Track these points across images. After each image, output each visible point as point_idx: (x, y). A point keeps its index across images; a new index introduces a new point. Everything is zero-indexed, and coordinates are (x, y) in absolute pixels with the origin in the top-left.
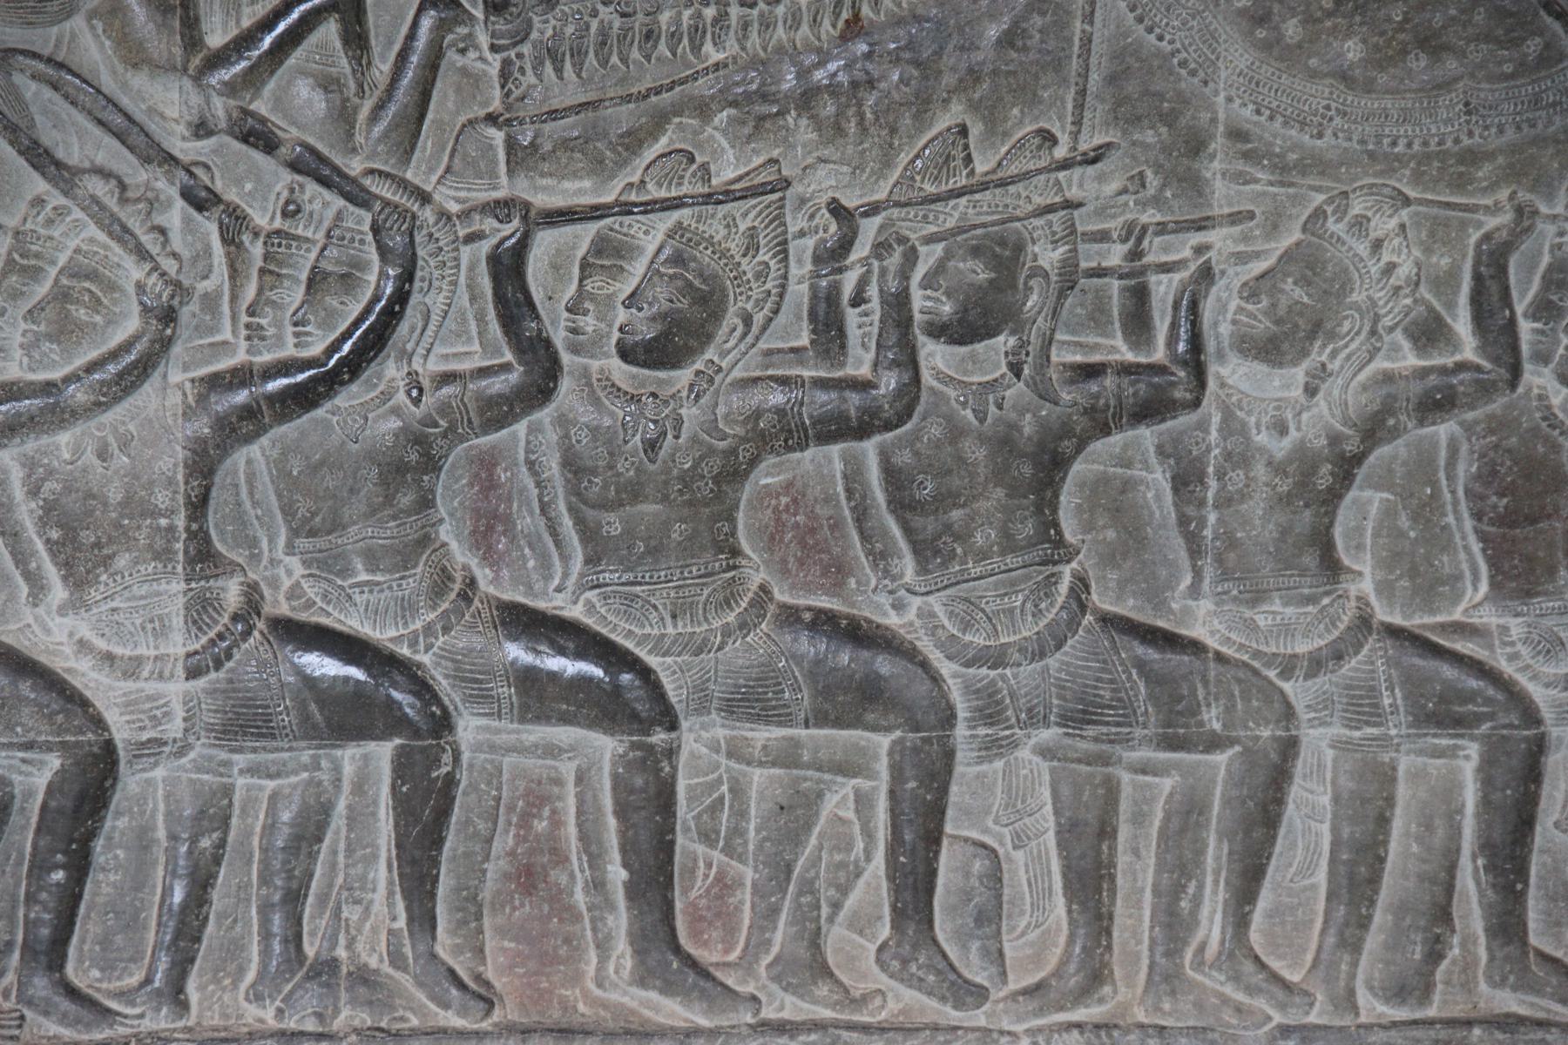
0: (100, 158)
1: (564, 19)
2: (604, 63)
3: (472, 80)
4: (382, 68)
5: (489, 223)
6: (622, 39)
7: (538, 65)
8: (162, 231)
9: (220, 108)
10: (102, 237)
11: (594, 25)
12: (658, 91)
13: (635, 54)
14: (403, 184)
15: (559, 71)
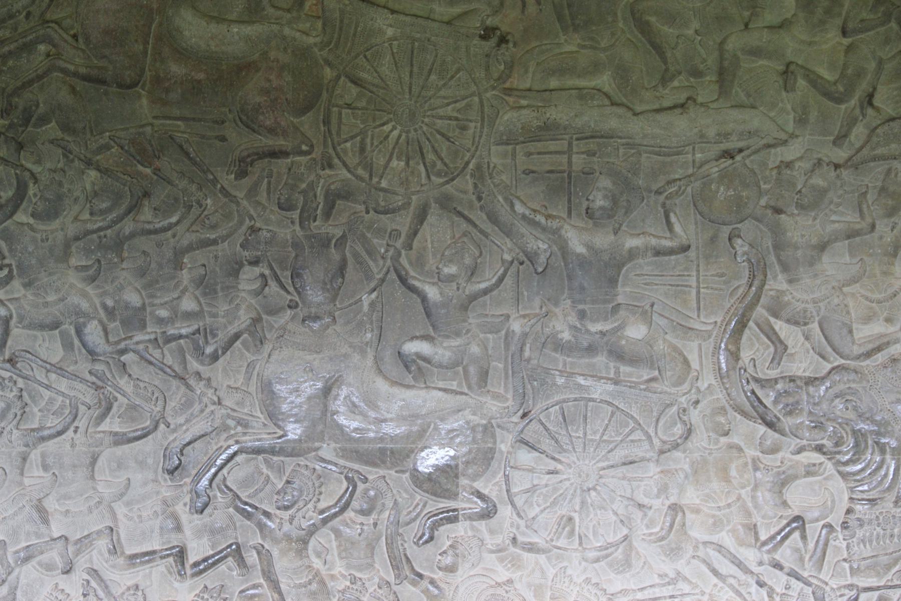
0: (731, 572)
1: (866, 531)
2: (878, 544)
3: (837, 549)
4: (811, 545)
5: (847, 591)
6: (883, 537)
7: (858, 544)
8: (750, 593)
9: (766, 557)
10: (734, 595)
11: (875, 533)
12: (895, 552)
13: (888, 541)
14: (820, 580)
15: (865, 546)
